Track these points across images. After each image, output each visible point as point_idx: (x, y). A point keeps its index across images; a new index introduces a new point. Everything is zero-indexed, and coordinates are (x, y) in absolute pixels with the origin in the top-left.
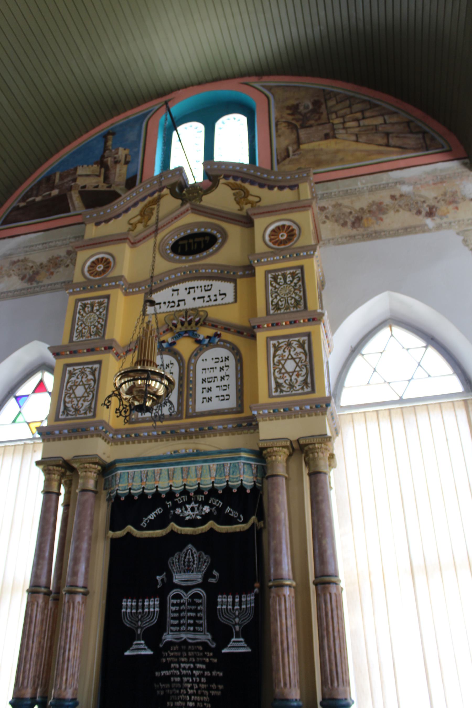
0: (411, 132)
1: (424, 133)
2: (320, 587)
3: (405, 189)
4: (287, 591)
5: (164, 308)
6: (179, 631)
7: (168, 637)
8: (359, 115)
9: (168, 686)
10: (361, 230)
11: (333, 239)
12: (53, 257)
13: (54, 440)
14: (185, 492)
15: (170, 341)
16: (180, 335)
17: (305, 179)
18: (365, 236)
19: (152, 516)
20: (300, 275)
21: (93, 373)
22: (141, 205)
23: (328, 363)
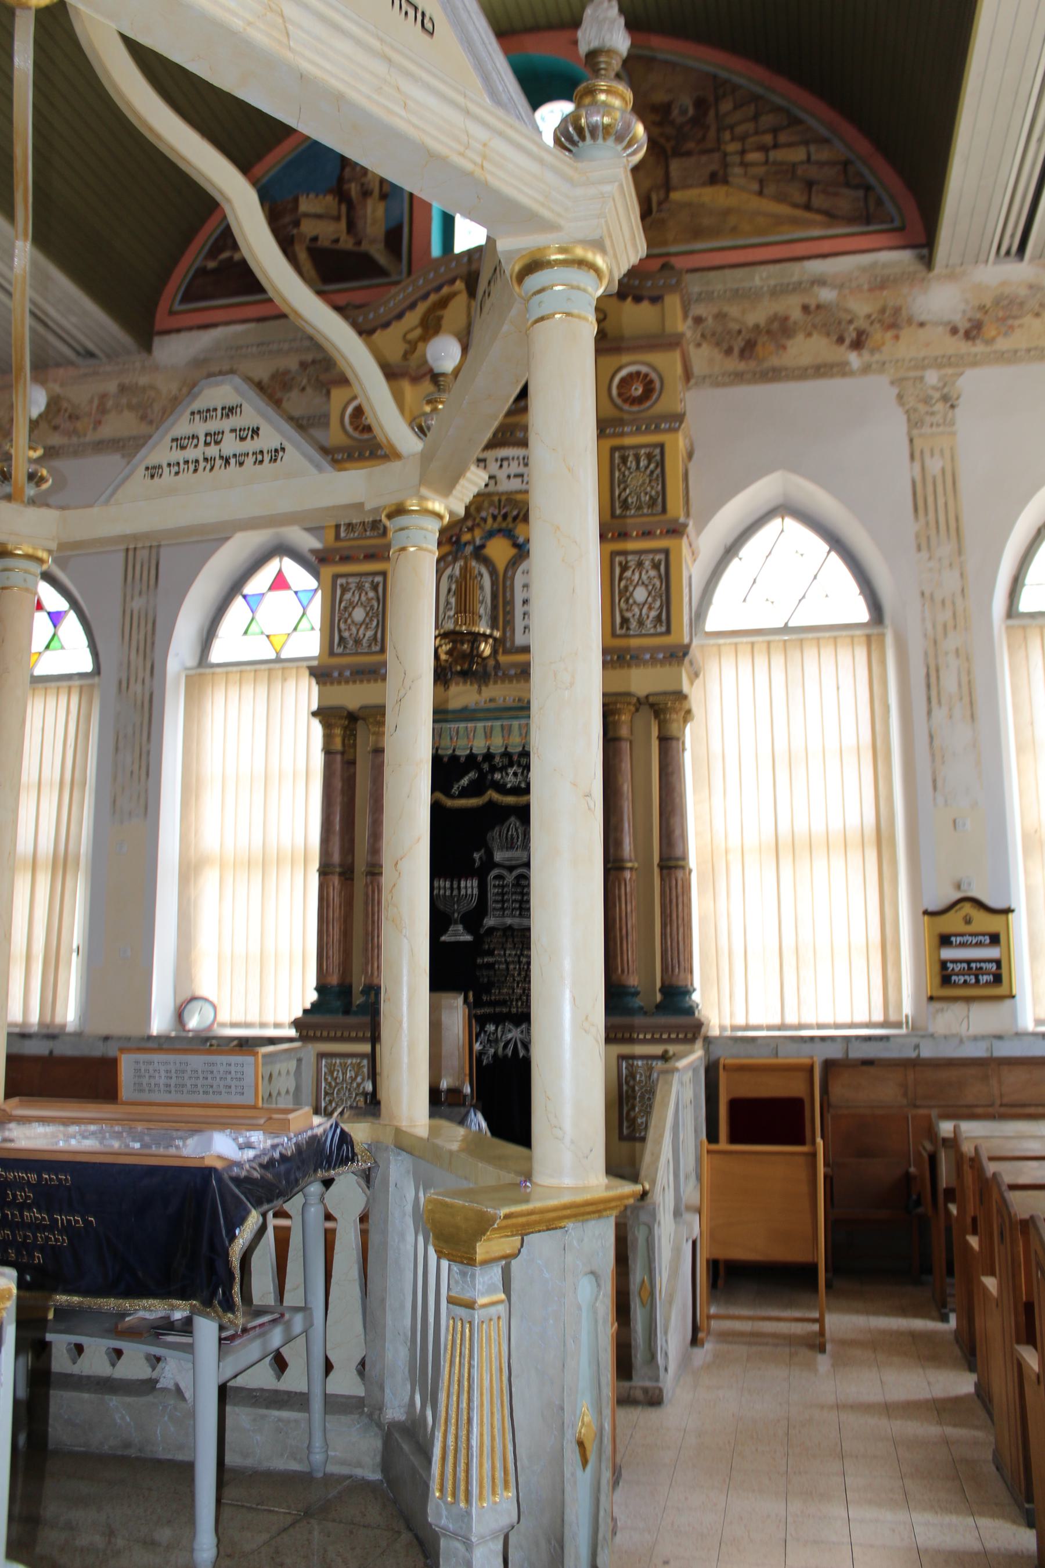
0: (848, 185)
1: (868, 188)
2: (665, 872)
3: (826, 295)
4: (627, 875)
6: (503, 916)
7: (490, 921)
8: (768, 139)
9: (492, 973)
10: (752, 364)
11: (710, 376)
12: (277, 371)
13: (332, 683)
14: (506, 754)
15: (478, 542)
16: (490, 534)
17: (676, 288)
18: (757, 376)
19: (465, 781)
20: (658, 457)
21: (375, 588)
22: (422, 308)
23: (690, 578)
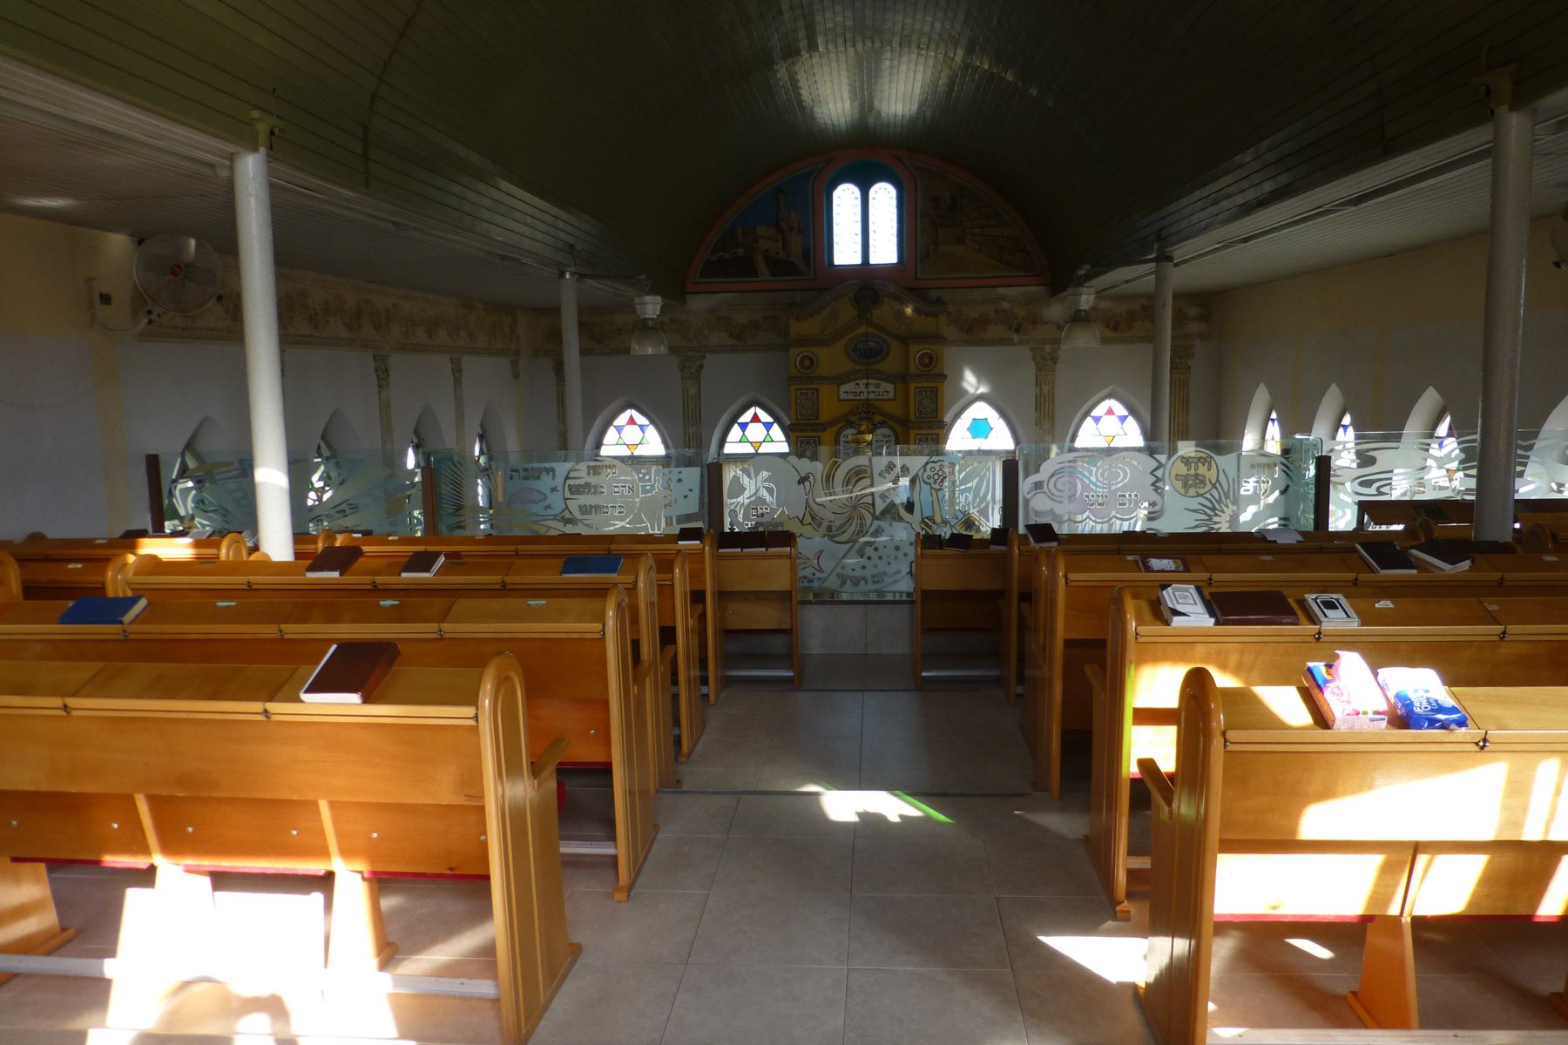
3: (1006, 305)
5: (851, 397)
